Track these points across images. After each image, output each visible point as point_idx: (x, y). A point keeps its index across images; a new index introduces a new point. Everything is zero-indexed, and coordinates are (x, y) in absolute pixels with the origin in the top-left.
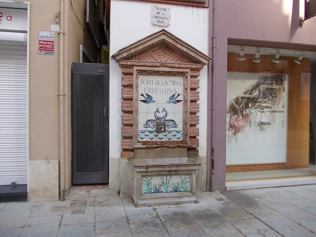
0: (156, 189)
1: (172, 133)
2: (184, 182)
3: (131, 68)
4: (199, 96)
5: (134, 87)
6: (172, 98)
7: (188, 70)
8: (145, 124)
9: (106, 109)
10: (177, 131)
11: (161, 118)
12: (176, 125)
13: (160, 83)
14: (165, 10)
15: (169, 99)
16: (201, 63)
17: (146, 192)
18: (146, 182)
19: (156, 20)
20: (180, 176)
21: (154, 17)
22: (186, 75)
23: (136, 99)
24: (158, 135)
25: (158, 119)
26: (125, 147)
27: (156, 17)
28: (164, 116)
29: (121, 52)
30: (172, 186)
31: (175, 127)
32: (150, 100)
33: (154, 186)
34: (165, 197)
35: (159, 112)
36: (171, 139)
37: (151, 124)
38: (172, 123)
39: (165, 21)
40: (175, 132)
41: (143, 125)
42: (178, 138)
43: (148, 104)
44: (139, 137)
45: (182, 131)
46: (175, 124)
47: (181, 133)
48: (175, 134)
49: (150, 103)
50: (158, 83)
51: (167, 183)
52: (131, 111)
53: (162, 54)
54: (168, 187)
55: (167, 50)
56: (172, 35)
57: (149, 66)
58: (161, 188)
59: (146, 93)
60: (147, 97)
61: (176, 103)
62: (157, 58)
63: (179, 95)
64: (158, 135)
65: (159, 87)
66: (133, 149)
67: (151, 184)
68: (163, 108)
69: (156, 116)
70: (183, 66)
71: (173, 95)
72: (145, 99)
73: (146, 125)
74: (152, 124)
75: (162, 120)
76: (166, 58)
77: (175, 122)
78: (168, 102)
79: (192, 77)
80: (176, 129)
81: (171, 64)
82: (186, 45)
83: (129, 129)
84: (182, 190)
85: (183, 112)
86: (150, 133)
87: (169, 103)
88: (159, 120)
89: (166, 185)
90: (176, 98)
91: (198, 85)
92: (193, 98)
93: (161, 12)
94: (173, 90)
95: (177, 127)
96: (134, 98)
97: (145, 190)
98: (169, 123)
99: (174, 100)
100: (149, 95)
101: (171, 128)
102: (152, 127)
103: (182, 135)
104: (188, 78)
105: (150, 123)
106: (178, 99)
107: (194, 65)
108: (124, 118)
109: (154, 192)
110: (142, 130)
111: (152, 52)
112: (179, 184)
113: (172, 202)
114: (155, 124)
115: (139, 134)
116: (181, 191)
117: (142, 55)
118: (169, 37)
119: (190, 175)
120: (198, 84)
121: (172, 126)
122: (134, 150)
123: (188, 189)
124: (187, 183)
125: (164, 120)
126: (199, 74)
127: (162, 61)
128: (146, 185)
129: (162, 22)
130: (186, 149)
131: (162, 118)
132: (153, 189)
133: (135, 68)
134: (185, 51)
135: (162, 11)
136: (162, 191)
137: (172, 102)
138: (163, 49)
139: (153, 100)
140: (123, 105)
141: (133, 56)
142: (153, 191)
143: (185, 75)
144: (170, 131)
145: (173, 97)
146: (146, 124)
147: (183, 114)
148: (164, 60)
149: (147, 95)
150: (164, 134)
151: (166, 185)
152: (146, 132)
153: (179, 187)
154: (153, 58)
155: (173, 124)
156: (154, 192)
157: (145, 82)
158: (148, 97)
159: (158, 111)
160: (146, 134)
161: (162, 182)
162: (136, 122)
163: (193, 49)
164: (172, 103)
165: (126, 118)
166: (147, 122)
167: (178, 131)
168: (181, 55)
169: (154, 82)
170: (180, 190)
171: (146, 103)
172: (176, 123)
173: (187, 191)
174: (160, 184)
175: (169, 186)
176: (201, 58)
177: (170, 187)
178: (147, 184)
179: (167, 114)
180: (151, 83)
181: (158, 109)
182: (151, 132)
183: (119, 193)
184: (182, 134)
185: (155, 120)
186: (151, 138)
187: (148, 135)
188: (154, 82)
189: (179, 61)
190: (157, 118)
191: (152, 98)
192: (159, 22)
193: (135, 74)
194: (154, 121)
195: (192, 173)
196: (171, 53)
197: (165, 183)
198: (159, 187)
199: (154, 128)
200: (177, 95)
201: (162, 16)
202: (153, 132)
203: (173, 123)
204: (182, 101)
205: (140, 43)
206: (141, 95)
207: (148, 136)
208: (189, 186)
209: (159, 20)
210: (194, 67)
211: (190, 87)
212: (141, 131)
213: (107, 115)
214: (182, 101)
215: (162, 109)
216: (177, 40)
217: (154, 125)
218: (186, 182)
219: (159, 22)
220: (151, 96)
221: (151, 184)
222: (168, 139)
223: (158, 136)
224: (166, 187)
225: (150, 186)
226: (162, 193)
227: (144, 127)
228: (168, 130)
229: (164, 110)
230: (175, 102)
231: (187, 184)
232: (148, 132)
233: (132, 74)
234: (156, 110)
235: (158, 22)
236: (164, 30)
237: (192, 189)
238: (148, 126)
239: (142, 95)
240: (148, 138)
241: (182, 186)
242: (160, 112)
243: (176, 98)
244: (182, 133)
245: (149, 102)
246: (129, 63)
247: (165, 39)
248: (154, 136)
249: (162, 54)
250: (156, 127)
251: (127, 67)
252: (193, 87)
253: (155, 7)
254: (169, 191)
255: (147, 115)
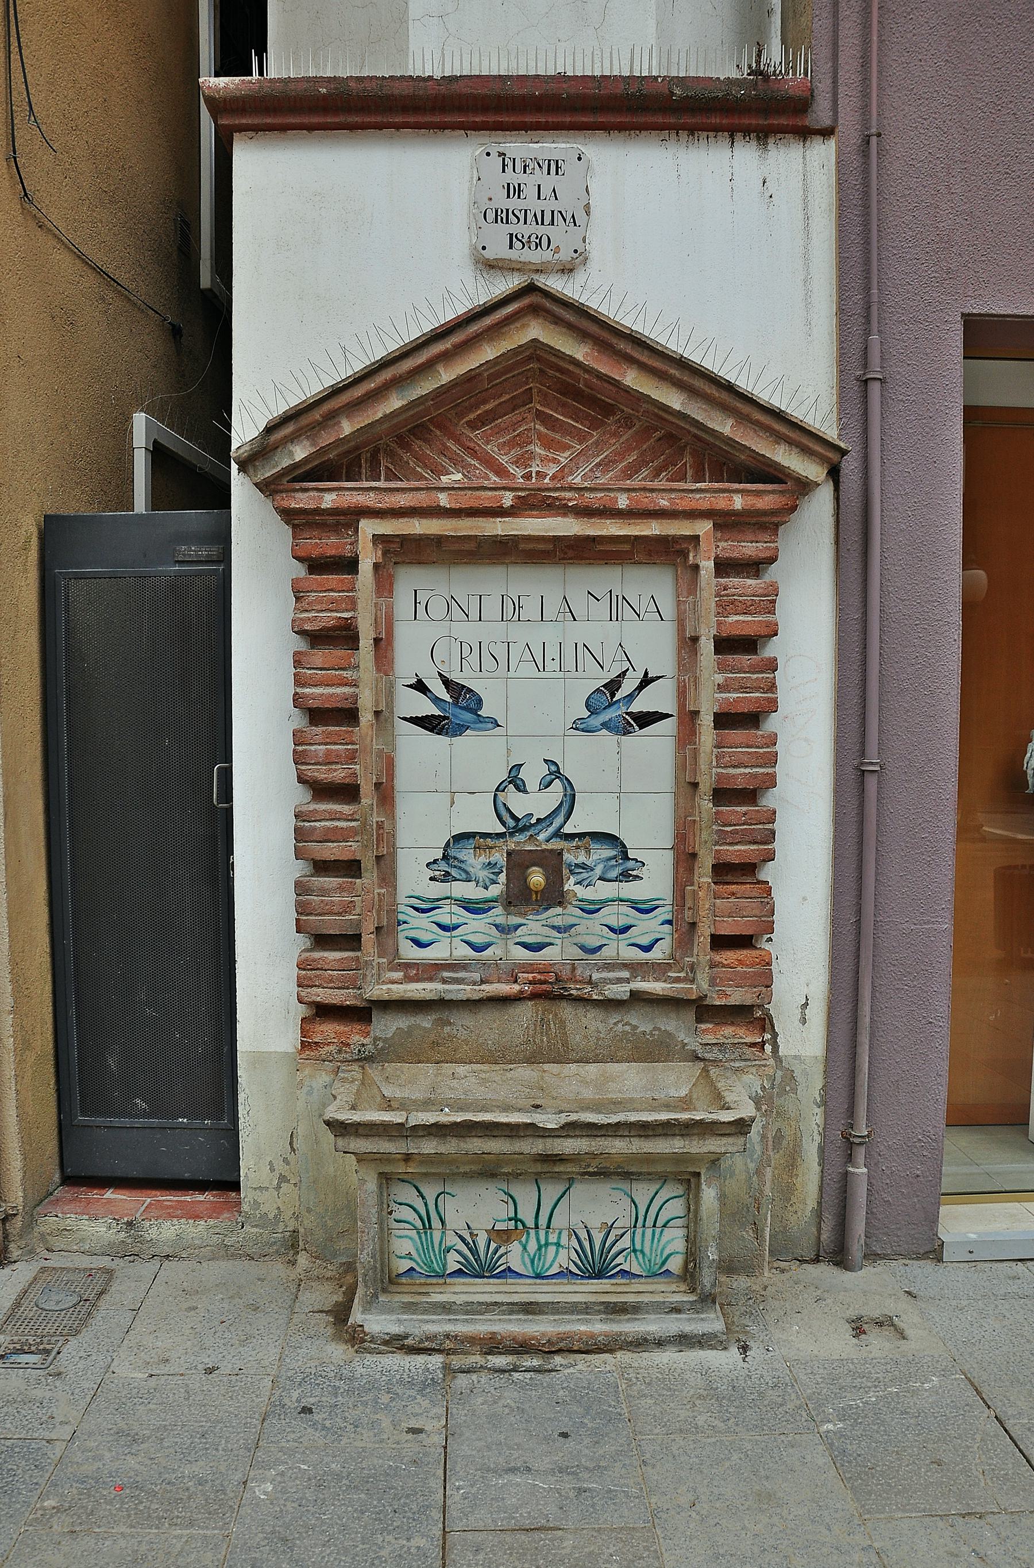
0: (474, 1251)
1: (612, 915)
2: (650, 1222)
3: (348, 526)
4: (772, 687)
5: (366, 642)
7: (703, 528)
8: (435, 861)
11: (533, 821)
13: (530, 610)
14: (555, 167)
15: (587, 706)
18: (415, 1210)
19: (503, 231)
20: (625, 1186)
21: (491, 216)
23: (377, 714)
24: (517, 927)
25: (520, 826)
27: (502, 217)
31: (626, 876)
32: (468, 716)
35: (521, 788)
37: (473, 861)
38: (603, 852)
39: (557, 233)
40: (625, 909)
41: (428, 865)
42: (645, 941)
44: (401, 936)
47: (664, 913)
48: (623, 922)
50: (518, 607)
51: (543, 1221)
52: (347, 781)
54: (547, 1244)
55: (564, 405)
59: (440, 675)
60: (447, 697)
62: (503, 460)
63: (646, 681)
65: (519, 634)
66: (364, 1004)
69: (501, 811)
70: (664, 503)
71: (612, 681)
72: (437, 712)
73: (443, 866)
75: (542, 837)
76: (564, 457)
77: (624, 846)
78: (580, 726)
79: (724, 567)
80: (630, 890)
83: (341, 888)
84: (636, 1270)
85: (677, 783)
87: (583, 730)
88: (521, 838)
89: (532, 1232)
90: (631, 697)
91: (770, 618)
93: (530, 182)
102: (483, 874)
104: (703, 572)
105: (466, 854)
107: (737, 491)
108: (307, 824)
109: (459, 1273)
111: (473, 425)
114: (499, 857)
115: (401, 917)
116: (624, 1273)
117: (417, 445)
121: (606, 870)
122: (371, 1008)
124: (664, 1226)
125: (558, 834)
127: (538, 473)
128: (416, 1228)
131: (538, 820)
132: (453, 1256)
133: (368, 528)
134: (677, 406)
135: (538, 176)
137: (605, 725)
140: (300, 748)
142: (453, 1266)
143: (685, 554)
144: (592, 902)
145: (613, 695)
146: (445, 857)
148: (552, 470)
149: (447, 683)
150: (558, 922)
151: (532, 1232)
152: (447, 909)
155: (614, 857)
156: (459, 1273)
157: (438, 608)
159: (515, 780)
160: (446, 920)
161: (512, 1215)
163: (724, 396)
164: (604, 732)
165: (317, 824)
166: (448, 844)
167: (645, 902)
169: (492, 607)
175: (553, 1238)
180: (474, 615)
182: (472, 907)
184: (669, 922)
185: (500, 836)
186: (478, 939)
187: (456, 927)
189: (645, 472)
190: (511, 823)
191: (480, 702)
192: (518, 245)
193: (366, 566)
195: (699, 1174)
196: (595, 425)
198: (493, 1245)
199: (494, 882)
201: (536, 206)
202: (490, 909)
203: (613, 853)
204: (667, 716)
205: (386, 375)
207: (455, 933)
210: (738, 503)
214: (667, 716)
216: (622, 345)
218: (659, 1223)
219: (518, 245)
220: (470, 691)
222: (583, 948)
223: (519, 932)
224: (532, 1246)
225: (437, 1235)
227: (431, 879)
228: (581, 892)
229: (556, 773)
233: (351, 565)
235: (511, 247)
238: (454, 872)
239: (420, 686)
240: (457, 941)
241: (638, 1247)
242: (532, 785)
243: (631, 697)
244: (669, 917)
245: (459, 730)
246: (329, 500)
249: (540, 437)
250: (502, 878)
251: (323, 526)
253: (494, 154)
255: (452, 803)
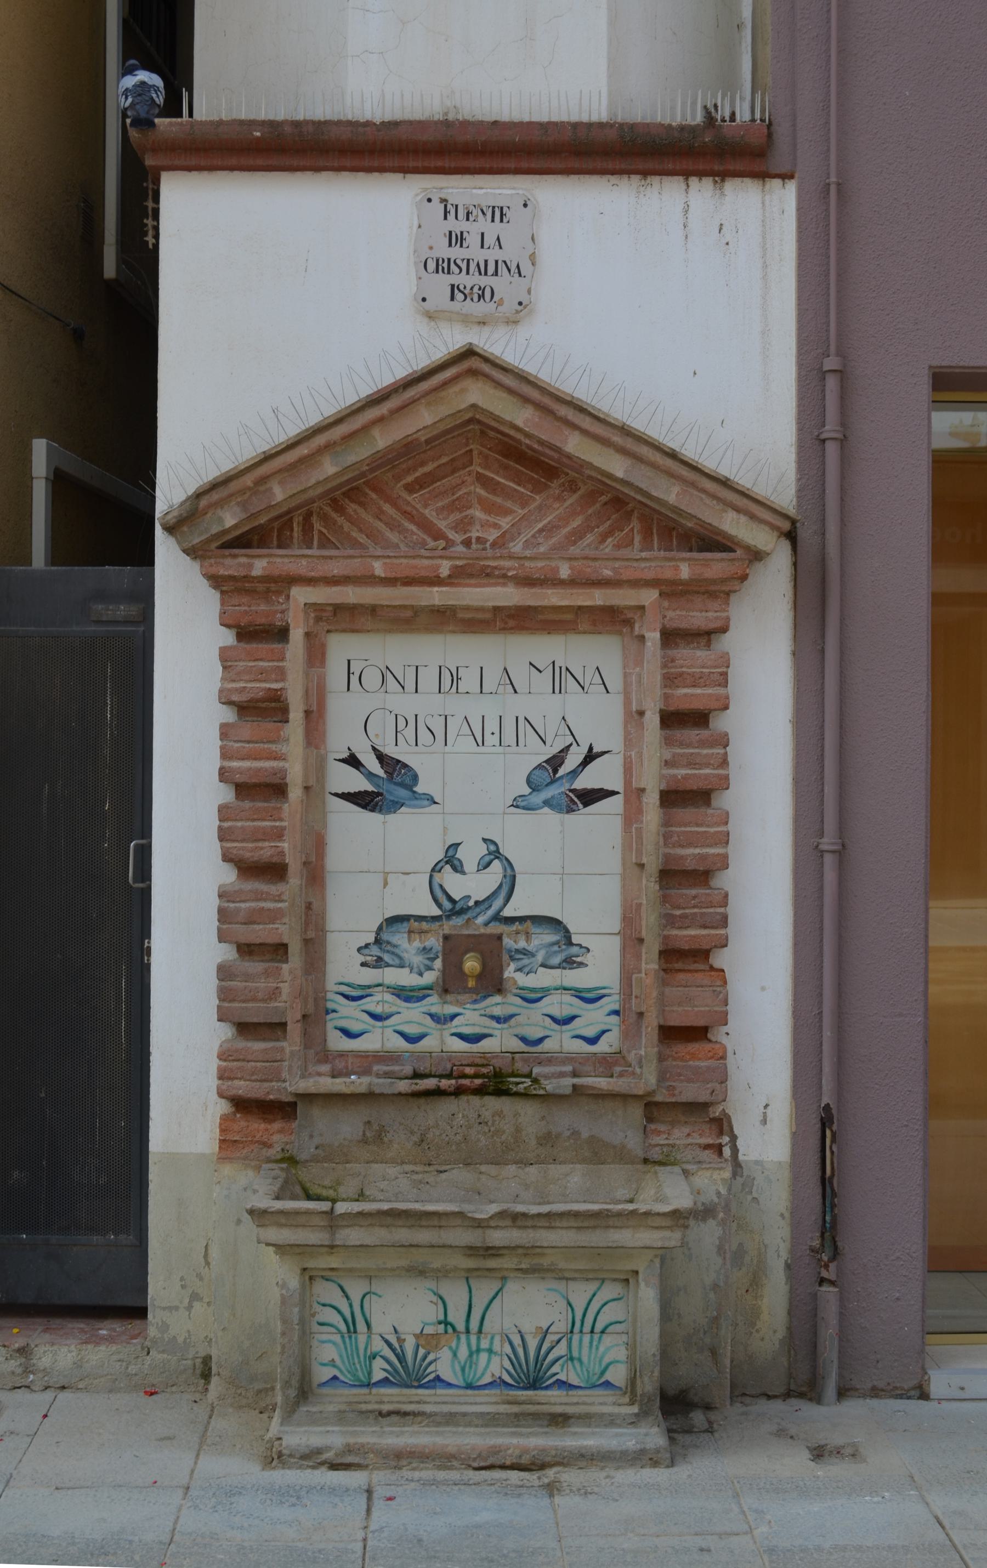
0: (401, 1358)
1: (557, 1005)
2: (587, 1328)
3: (279, 593)
4: (724, 763)
5: (296, 715)
6: (545, 776)
7: (649, 597)
8: (367, 946)
9: (136, 846)
10: (577, 990)
11: (471, 903)
12: (575, 950)
13: (469, 681)
14: (499, 214)
15: (529, 782)
16: (733, 551)
17: (386, 1379)
18: (339, 1312)
19: (444, 281)
20: (561, 1286)
21: (431, 265)
22: (637, 626)
23: (307, 789)
24: (453, 1017)
25: (456, 909)
26: (242, 1088)
27: (443, 266)
28: (494, 894)
29: (203, 502)
30: (508, 1349)
31: (570, 963)
32: (402, 793)
33: (387, 1342)
34: (451, 1419)
35: (458, 868)
36: (541, 1040)
37: (408, 946)
38: (542, 938)
39: (502, 282)
40: (568, 998)
41: (359, 950)
42: (590, 1032)
43: (391, 817)
44: (330, 1026)
45: (616, 989)
46: (570, 943)
47: (611, 1003)
48: (567, 1012)
49: (403, 809)
50: (455, 679)
51: (474, 1325)
52: (274, 860)
53: (481, 500)
54: (478, 1350)
55: (506, 468)
56: (523, 377)
57: (390, 582)
58: (431, 1357)
59: (374, 749)
60: (380, 772)
61: (570, 810)
62: (442, 525)
63: (590, 757)
64: (453, 1017)
65: (456, 706)
66: (290, 1099)
67: (369, 1326)
68: (485, 840)
69: (437, 892)
70: (607, 573)
71: (554, 757)
72: (370, 788)
73: (375, 951)
74: (417, 944)
75: (480, 920)
76: (505, 523)
77: (567, 931)
78: (518, 804)
79: (670, 637)
80: (573, 978)
81: (527, 564)
82: (617, 439)
83: (267, 974)
84: (574, 1380)
85: (624, 864)
86: (398, 1001)
87: (524, 808)
88: (458, 921)
89: (463, 1337)
90: (574, 773)
91: (721, 691)
92: (686, 777)
93: (472, 230)
94: (551, 728)
95: (581, 964)
96: (295, 773)
97: (332, 1363)
98: (528, 939)
99: (562, 787)
100: (398, 761)
101: (541, 970)
102: (417, 960)
103: (614, 1019)
104: (649, 644)
105: (399, 938)
106: (586, 781)
107: (684, 560)
108: (232, 905)
109: (385, 1382)
110: (346, 981)
111: (410, 488)
112: (551, 1338)
113: (495, 1450)
114: (434, 942)
115: (330, 1005)
116: (561, 1384)
117: (352, 507)
118: (510, 391)
119: (627, 1281)
120: (725, 684)
121: (549, 955)
122: (295, 1103)
123: (608, 1376)
124: (603, 1332)
125: (497, 918)
126: (728, 619)
127: (478, 539)
128: (339, 1332)
129: (481, 297)
130: (636, 1112)
131: (477, 903)
132: (379, 1364)
133: (301, 595)
134: (620, 474)
135: (483, 224)
136: (438, 1378)
137: (547, 803)
138: (487, 467)
139: (419, 789)
140: (226, 824)
141: (288, 525)
142: (378, 1375)
143: (629, 623)
144: (533, 990)
145: (555, 771)
146: (378, 941)
147: (624, 877)
148: (492, 535)
149: (381, 757)
150: (497, 1011)
151: (463, 1337)
152: (378, 997)
153: (551, 1357)
154: (418, 525)
155: (557, 943)
156: (385, 1382)
157: (372, 679)
158: (390, 774)
159: (451, 860)
160: (378, 1010)
161: (442, 1317)
162: (311, 934)
163: (669, 463)
164: (546, 810)
165: (243, 905)
166: (380, 929)
167: (589, 990)
168: (604, 498)
169: (428, 679)
170: (562, 1377)
171: (372, 810)
172: (575, 939)
173: (607, 1384)
174: (429, 1330)
175: (485, 1344)
176: (731, 515)
177: (490, 1351)
178: (343, 1328)
179: (514, 878)
180: (410, 686)
181: (456, 846)
182: (405, 994)
183: (206, 1375)
184: (616, 1013)
185: (435, 919)
186: (411, 1030)
187: (388, 1017)
188: (428, 679)
189: (589, 538)
190: (447, 905)
191: (415, 778)
192: (459, 296)
193: (297, 635)
194: (424, 925)
195: (637, 1272)
196: (538, 488)
197: (461, 1327)
198: (422, 1352)
199: (429, 968)
200: (580, 758)
201: (478, 255)
202: (424, 997)
203: (554, 938)
204: (613, 793)
205: (320, 440)
206: (343, 761)
207: (387, 1023)
208: (621, 1354)
209: (457, 279)
210: (685, 572)
211: (659, 705)
212: (344, 989)
213: (141, 885)
214: (613, 793)
215: (483, 849)
216: (563, 411)
217: (425, 950)
218: (599, 1327)
219: (459, 296)
220: (405, 766)
221: (369, 1326)
222: (523, 1039)
223: (456, 1021)
224: (463, 1353)
225: (362, 1339)
226: (439, 1391)
227: (363, 964)
228: (523, 980)
229: (495, 853)
230: (564, 800)
231: (608, 1340)
232: (389, 997)
233: (282, 634)
234: (441, 855)
235: (452, 298)
236: (469, 353)
237: (632, 1381)
238: (387, 958)
239: (353, 761)
240: (389, 1032)
241: (575, 1354)
242: (470, 864)
243: (574, 773)
244: (616, 1007)
245: (395, 806)
246: (259, 567)
247: (480, 404)
248: (428, 1021)
249: (481, 500)
250: (438, 964)
251: (251, 592)
252: (685, 706)
253: (436, 200)
254: (487, 1379)
255: (386, 884)
